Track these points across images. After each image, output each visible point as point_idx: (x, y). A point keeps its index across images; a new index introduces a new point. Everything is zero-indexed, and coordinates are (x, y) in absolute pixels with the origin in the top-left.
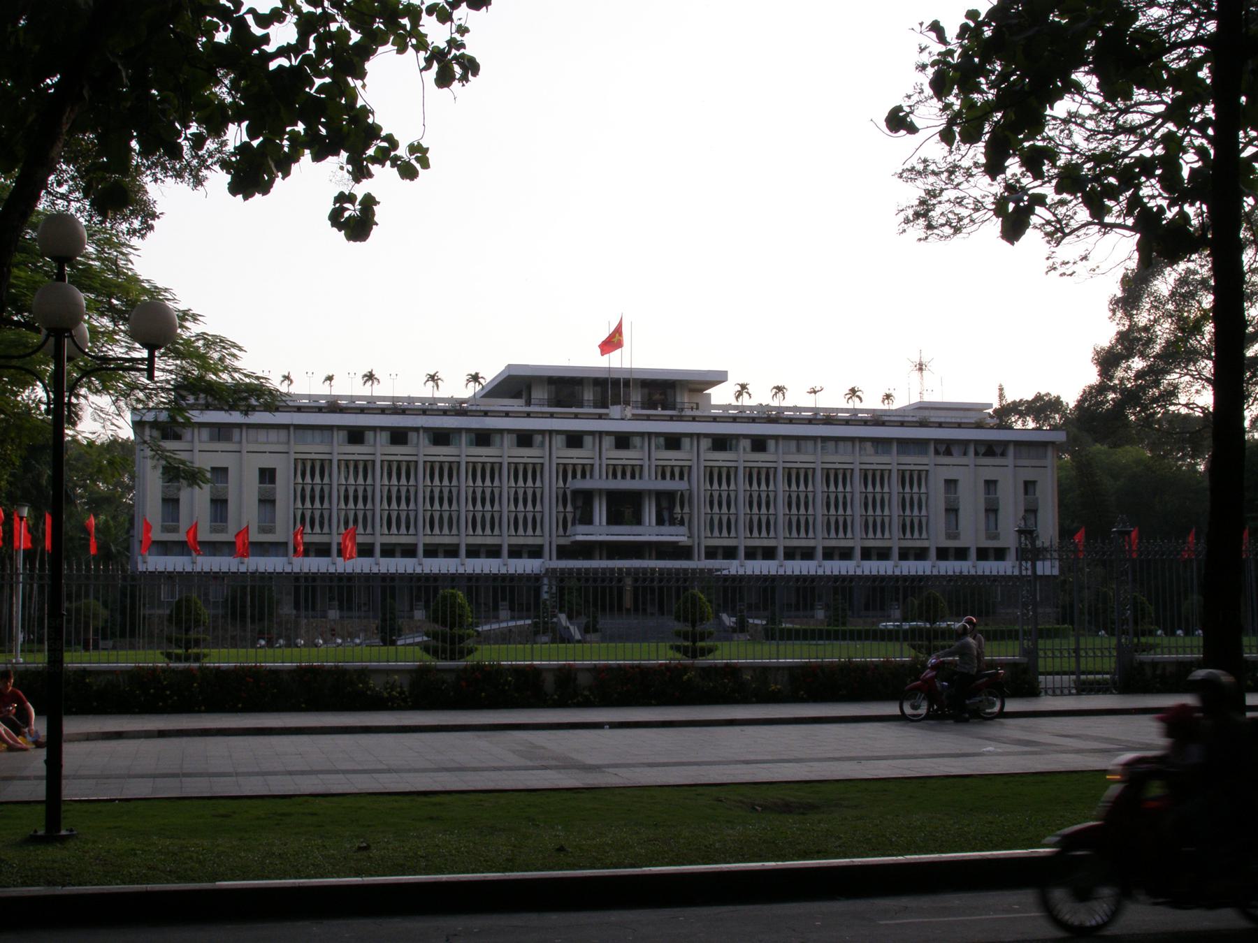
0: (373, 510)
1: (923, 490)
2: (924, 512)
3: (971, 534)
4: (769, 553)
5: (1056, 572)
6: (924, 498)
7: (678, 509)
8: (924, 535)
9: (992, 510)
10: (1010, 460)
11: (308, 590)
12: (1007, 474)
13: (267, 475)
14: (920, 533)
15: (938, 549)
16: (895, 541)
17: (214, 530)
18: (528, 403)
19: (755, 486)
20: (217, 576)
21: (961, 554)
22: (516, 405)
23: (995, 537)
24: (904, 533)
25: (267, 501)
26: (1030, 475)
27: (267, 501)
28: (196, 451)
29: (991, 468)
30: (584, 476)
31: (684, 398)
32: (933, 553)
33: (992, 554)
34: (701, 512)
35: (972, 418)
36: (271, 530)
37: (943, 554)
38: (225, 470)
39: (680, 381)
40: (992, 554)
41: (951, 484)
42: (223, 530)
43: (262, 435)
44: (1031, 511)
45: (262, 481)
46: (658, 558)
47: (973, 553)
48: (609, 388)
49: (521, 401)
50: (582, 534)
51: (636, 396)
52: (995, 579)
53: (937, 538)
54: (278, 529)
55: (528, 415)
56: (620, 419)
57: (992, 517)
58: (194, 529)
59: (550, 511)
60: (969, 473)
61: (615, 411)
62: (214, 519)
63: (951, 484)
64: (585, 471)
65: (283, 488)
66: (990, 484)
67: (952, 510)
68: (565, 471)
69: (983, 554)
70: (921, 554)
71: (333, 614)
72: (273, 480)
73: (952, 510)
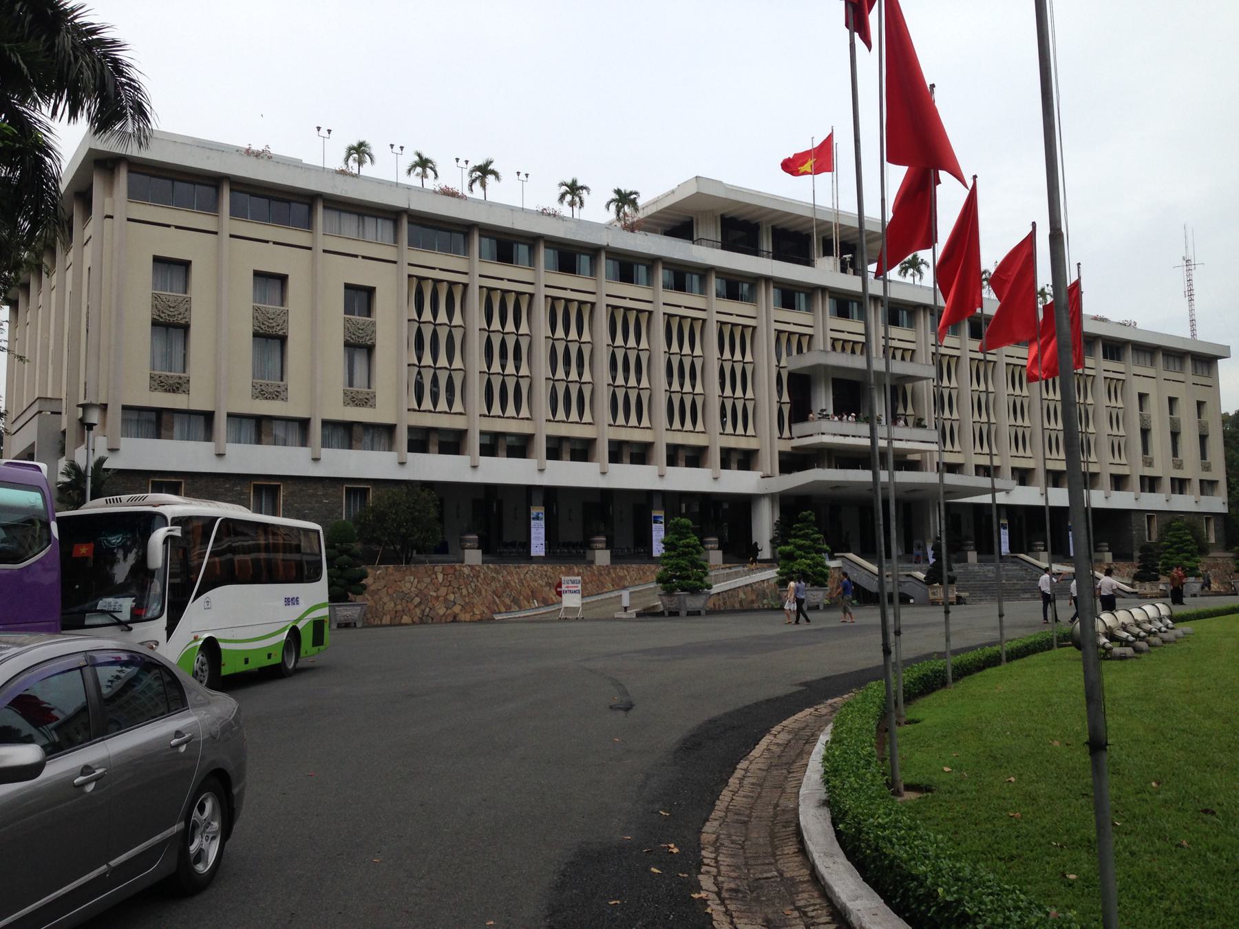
5: (1224, 509)
7: (901, 410)
13: (360, 298)
17: (262, 393)
25: (360, 347)
27: (360, 347)
28: (225, 234)
30: (800, 350)
36: (366, 401)
38: (283, 279)
41: (1142, 397)
43: (350, 223)
45: (348, 310)
54: (379, 399)
59: (767, 398)
62: (259, 371)
63: (1142, 397)
64: (802, 342)
67: (1145, 433)
71: (474, 556)
72: (369, 311)
73: (1145, 433)
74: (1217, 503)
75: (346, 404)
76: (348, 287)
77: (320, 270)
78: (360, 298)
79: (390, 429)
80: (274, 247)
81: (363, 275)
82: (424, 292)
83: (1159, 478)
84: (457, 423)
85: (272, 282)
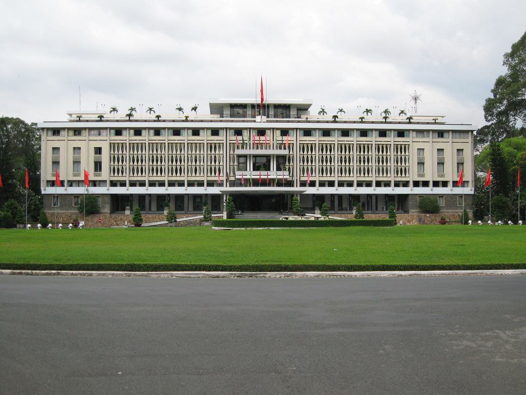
0: (293, 166)
1: (407, 154)
2: (407, 164)
3: (430, 175)
4: (331, 184)
5: (472, 193)
6: (407, 157)
8: (407, 175)
9: (441, 163)
10: (450, 140)
11: (119, 203)
12: (449, 145)
13: (98, 151)
14: (405, 175)
15: (413, 181)
16: (392, 178)
17: (75, 175)
18: (220, 117)
19: (381, 153)
20: (77, 196)
21: (426, 184)
22: (216, 117)
23: (443, 176)
24: (397, 174)
26: (460, 146)
29: (441, 143)
31: (293, 112)
32: (411, 184)
33: (441, 184)
34: (297, 165)
35: (430, 120)
37: (416, 184)
38: (80, 148)
39: (292, 104)
40: (441, 184)
42: (79, 175)
44: (460, 164)
45: (96, 153)
46: (254, 186)
47: (431, 184)
48: (262, 108)
49: (219, 116)
50: (239, 175)
51: (272, 112)
52: (441, 196)
53: (413, 176)
55: (221, 121)
56: (261, 122)
57: (442, 166)
58: (86, 176)
59: (224, 164)
60: (430, 146)
61: (258, 118)
65: (105, 158)
66: (440, 150)
67: (421, 163)
68: (233, 146)
69: (436, 184)
70: (406, 184)
72: (100, 153)
73: (421, 163)
74: (469, 190)
75: (94, 176)
76: (95, 148)
77: (87, 145)
78: (98, 151)
79: (106, 181)
80: (77, 142)
81: (98, 145)
82: (113, 146)
83: (429, 181)
84: (123, 179)
85: (77, 149)
